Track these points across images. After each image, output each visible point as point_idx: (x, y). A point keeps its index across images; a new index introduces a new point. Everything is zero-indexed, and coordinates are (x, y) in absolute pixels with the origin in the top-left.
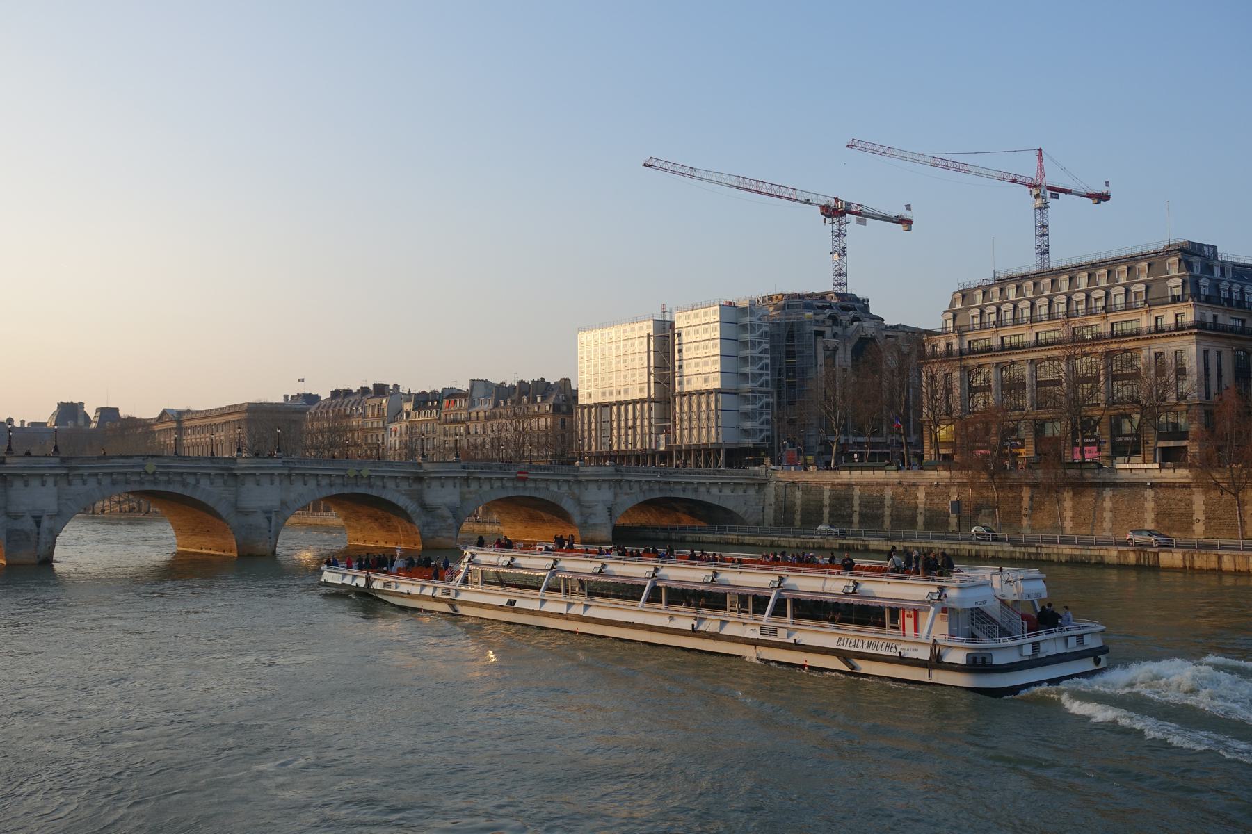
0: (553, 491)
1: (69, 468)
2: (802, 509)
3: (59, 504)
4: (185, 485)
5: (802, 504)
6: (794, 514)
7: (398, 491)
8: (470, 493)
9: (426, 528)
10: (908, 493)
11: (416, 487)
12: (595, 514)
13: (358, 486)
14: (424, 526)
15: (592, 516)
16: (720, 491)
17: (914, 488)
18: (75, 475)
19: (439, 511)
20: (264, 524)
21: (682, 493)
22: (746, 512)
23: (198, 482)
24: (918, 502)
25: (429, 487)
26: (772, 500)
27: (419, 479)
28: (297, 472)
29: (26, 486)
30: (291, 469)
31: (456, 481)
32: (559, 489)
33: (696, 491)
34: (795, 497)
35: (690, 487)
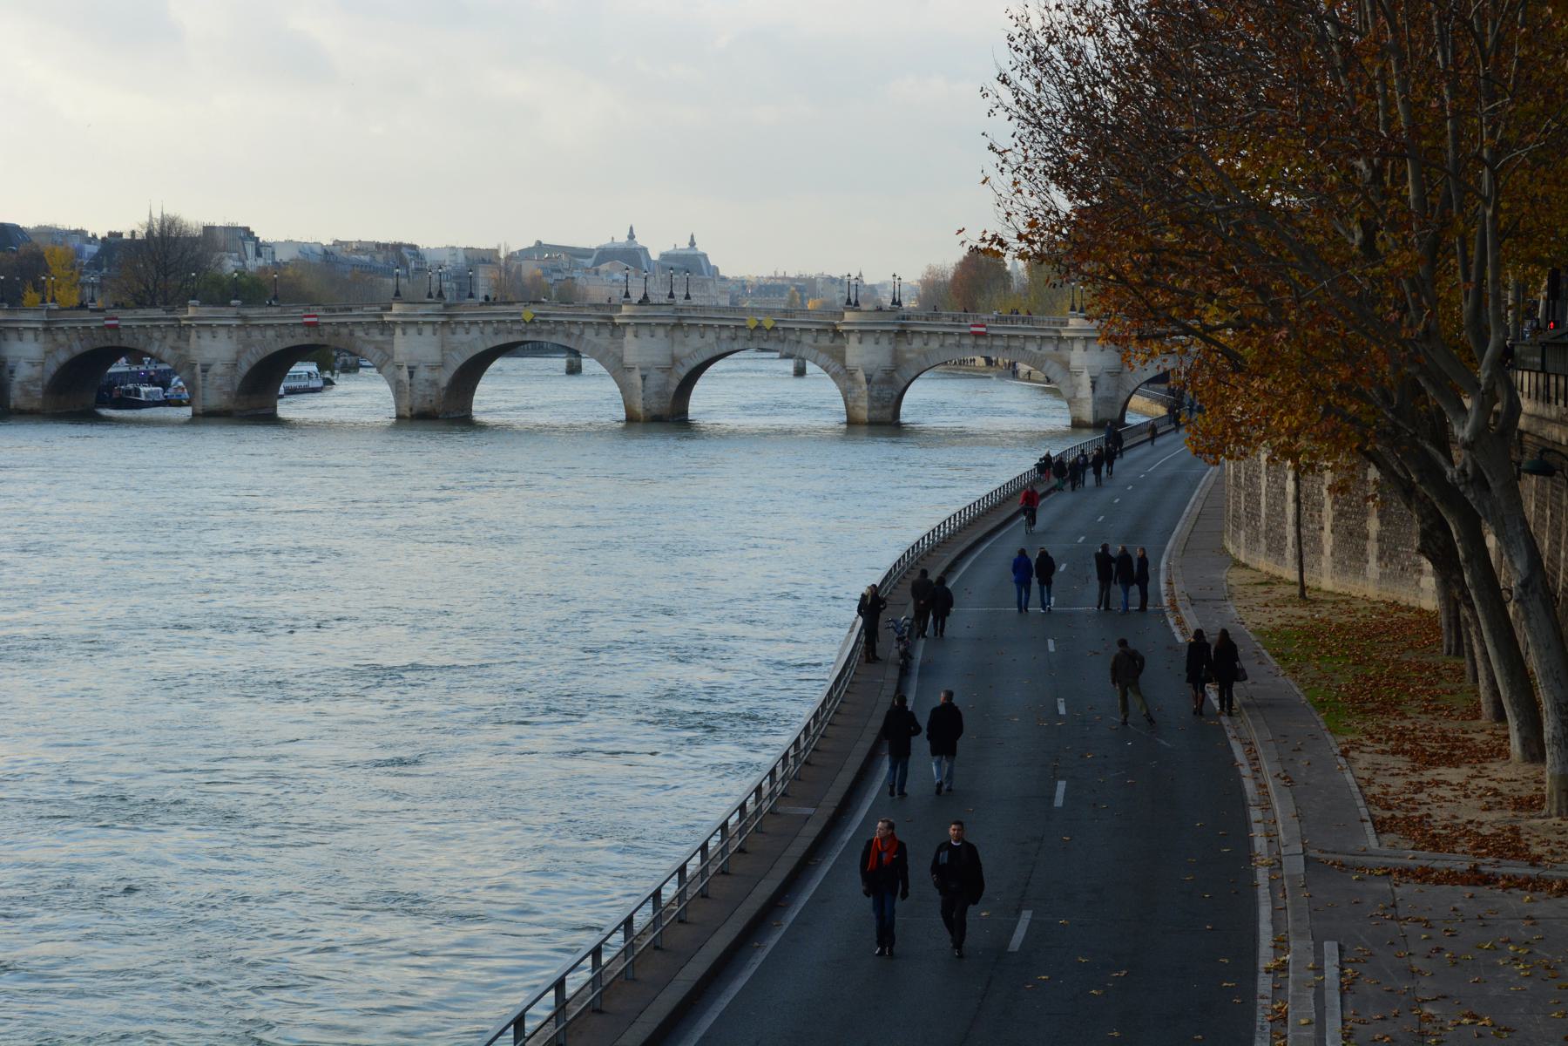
0: (1030, 351)
1: (450, 316)
3: (443, 355)
4: (569, 335)
7: (815, 348)
8: (911, 351)
11: (838, 342)
13: (765, 341)
18: (457, 323)
20: (639, 383)
23: (582, 333)
28: (689, 322)
29: (404, 334)
30: (680, 318)
32: (1040, 349)
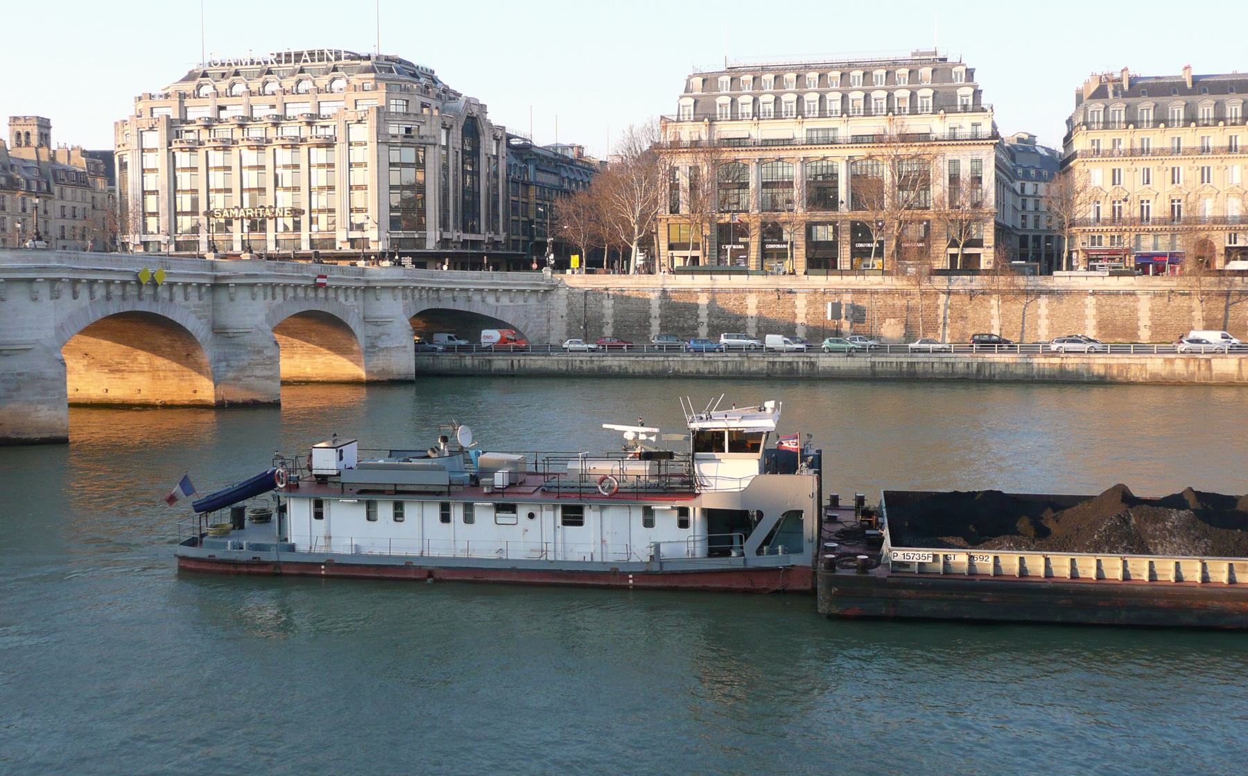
2: (615, 321)
5: (615, 315)
6: (601, 327)
9: (224, 364)
10: (781, 301)
12: (389, 335)
14: (219, 361)
15: (383, 337)
16: (497, 301)
17: (790, 296)
19: (247, 337)
21: (452, 303)
22: (526, 326)
24: (796, 311)
25: (232, 300)
26: (563, 310)
27: (217, 285)
31: (256, 289)
32: (346, 300)
33: (469, 299)
34: (602, 307)
35: (463, 294)
